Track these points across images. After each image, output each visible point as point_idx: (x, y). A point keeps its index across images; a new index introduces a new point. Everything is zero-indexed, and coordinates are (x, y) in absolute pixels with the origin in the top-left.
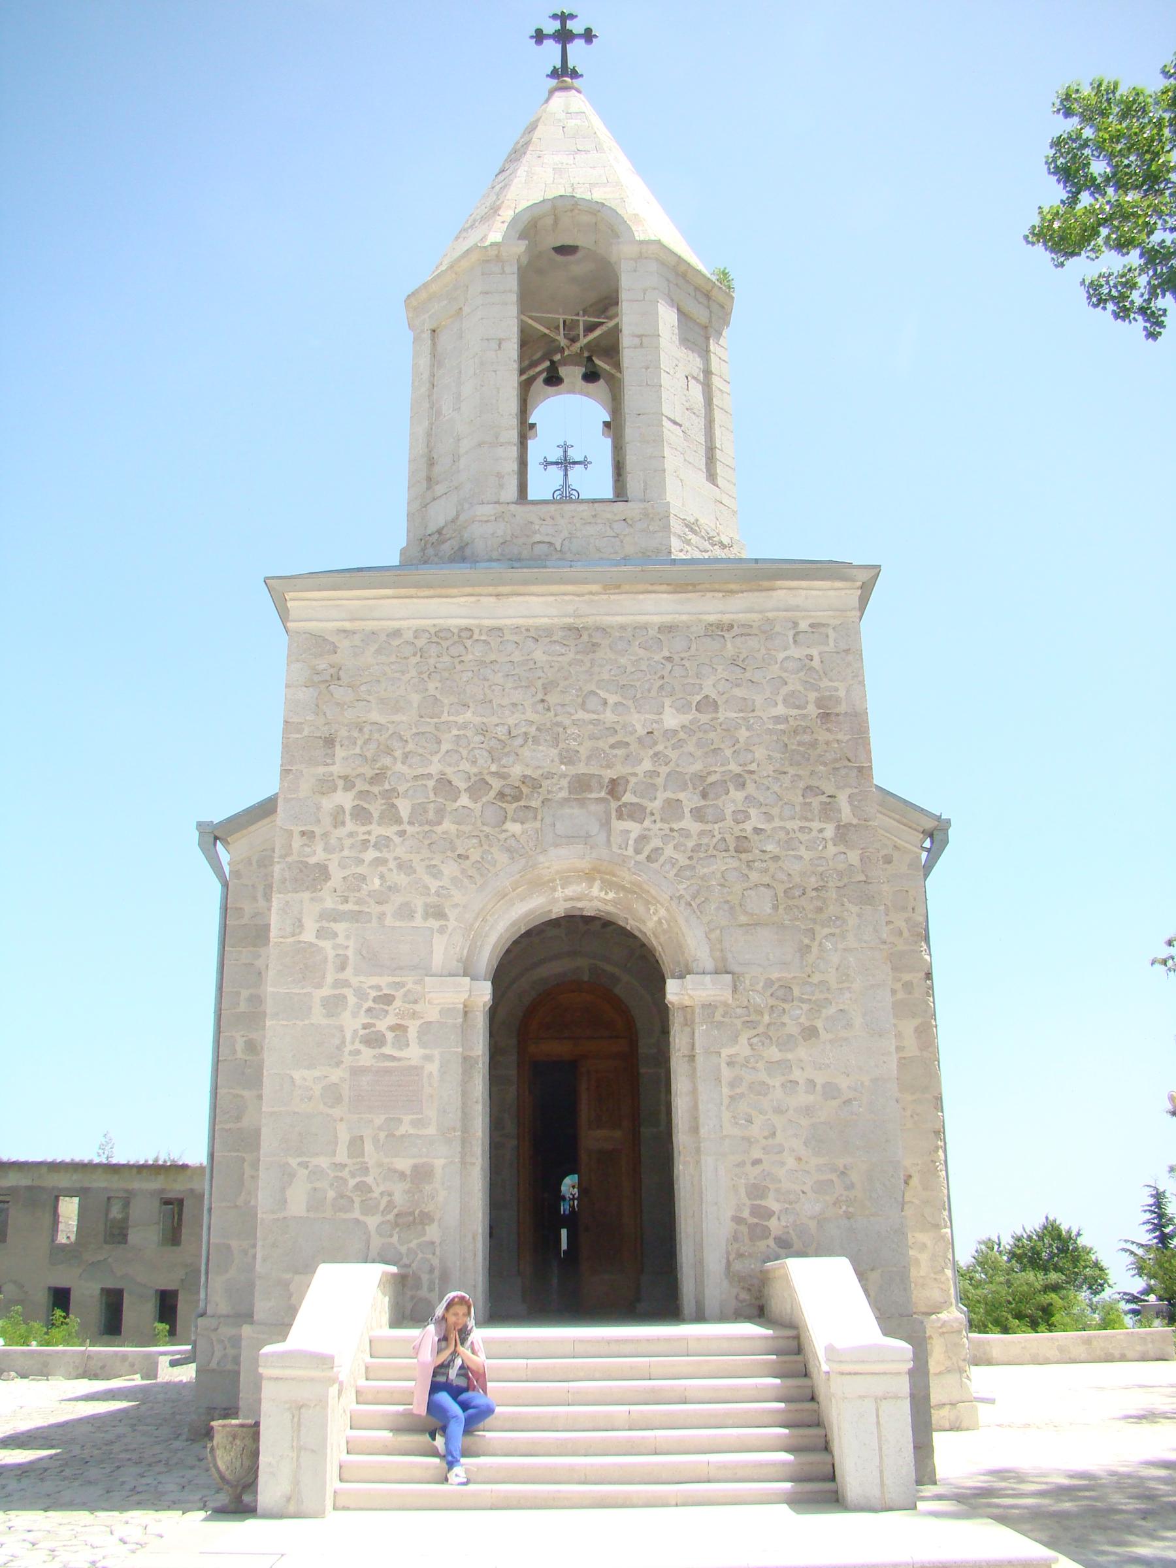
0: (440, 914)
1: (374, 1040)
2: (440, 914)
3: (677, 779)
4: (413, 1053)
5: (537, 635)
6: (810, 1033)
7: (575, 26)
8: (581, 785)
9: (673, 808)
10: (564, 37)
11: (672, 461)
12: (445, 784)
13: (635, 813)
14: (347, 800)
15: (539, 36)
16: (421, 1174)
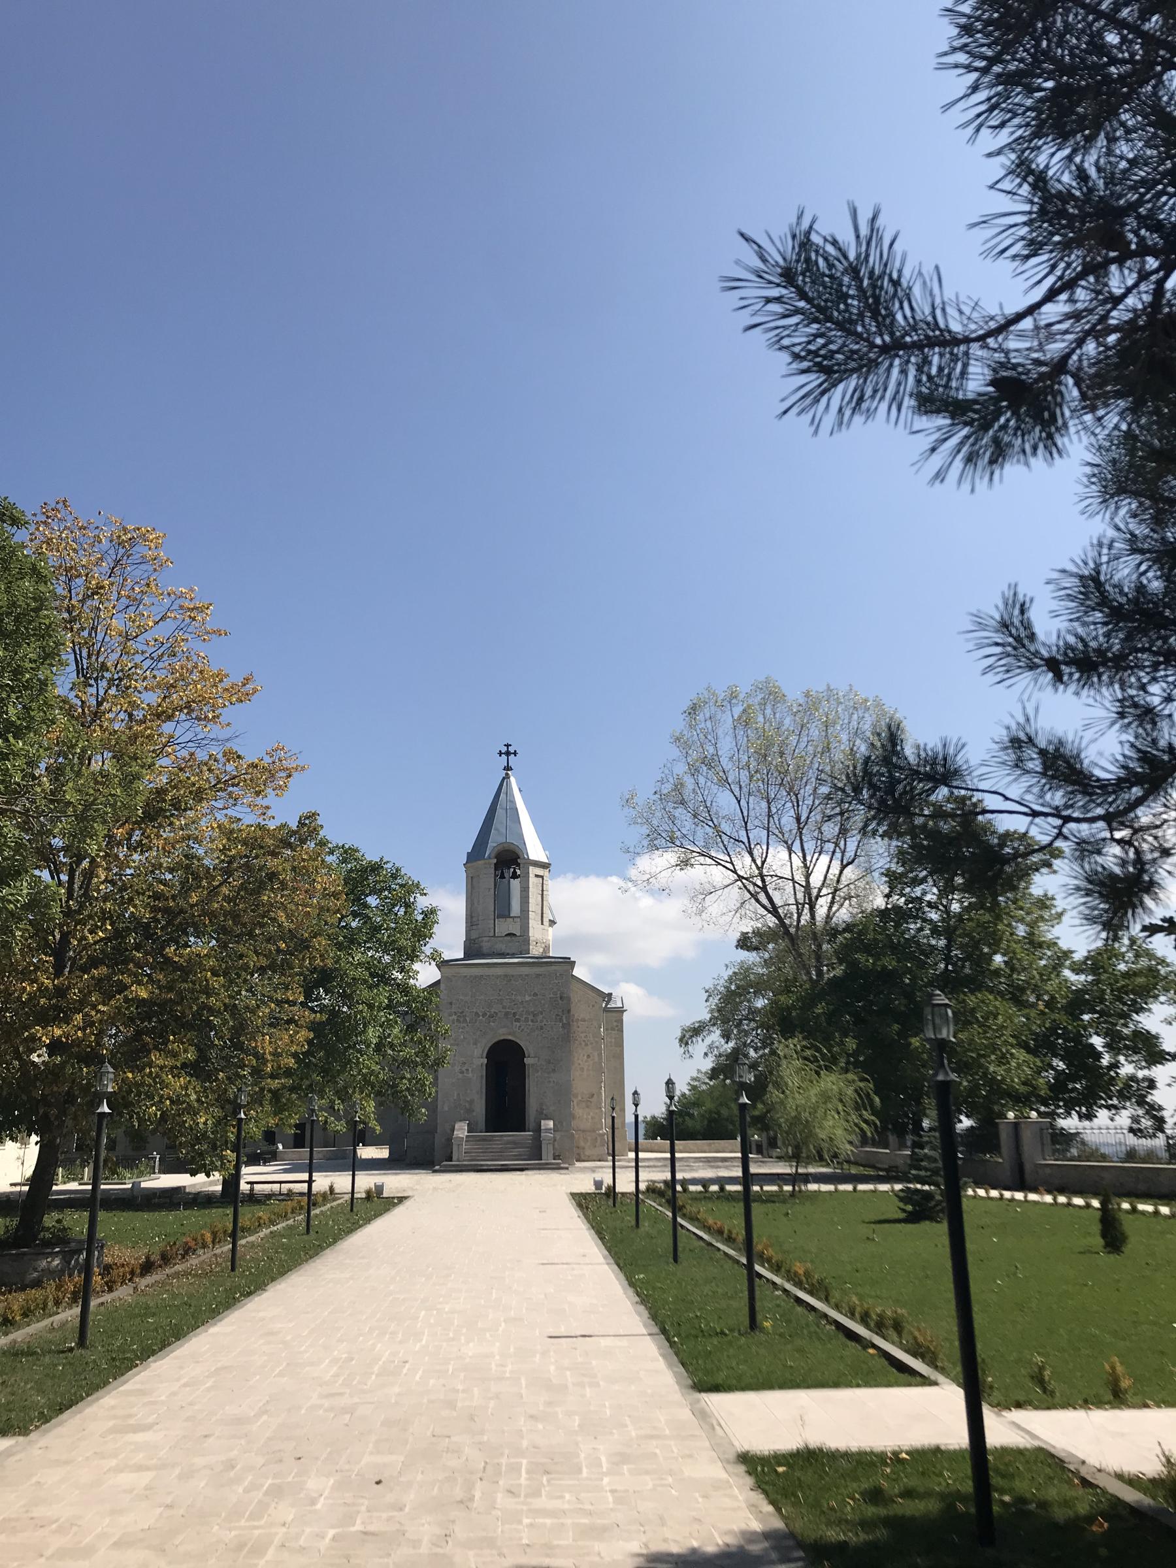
0: (475, 1044)
1: (462, 1072)
2: (475, 1044)
3: (528, 1013)
4: (470, 1075)
5: (498, 977)
6: (554, 1070)
7: (511, 749)
8: (507, 1014)
9: (527, 1020)
10: (508, 753)
11: (532, 923)
12: (477, 1014)
13: (518, 1020)
14: (455, 1017)
15: (500, 753)
16: (471, 1102)
